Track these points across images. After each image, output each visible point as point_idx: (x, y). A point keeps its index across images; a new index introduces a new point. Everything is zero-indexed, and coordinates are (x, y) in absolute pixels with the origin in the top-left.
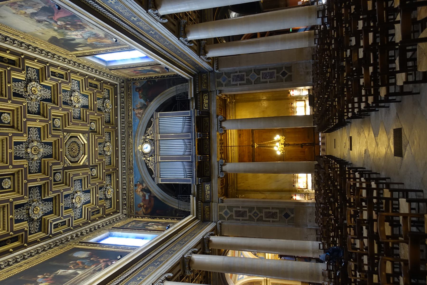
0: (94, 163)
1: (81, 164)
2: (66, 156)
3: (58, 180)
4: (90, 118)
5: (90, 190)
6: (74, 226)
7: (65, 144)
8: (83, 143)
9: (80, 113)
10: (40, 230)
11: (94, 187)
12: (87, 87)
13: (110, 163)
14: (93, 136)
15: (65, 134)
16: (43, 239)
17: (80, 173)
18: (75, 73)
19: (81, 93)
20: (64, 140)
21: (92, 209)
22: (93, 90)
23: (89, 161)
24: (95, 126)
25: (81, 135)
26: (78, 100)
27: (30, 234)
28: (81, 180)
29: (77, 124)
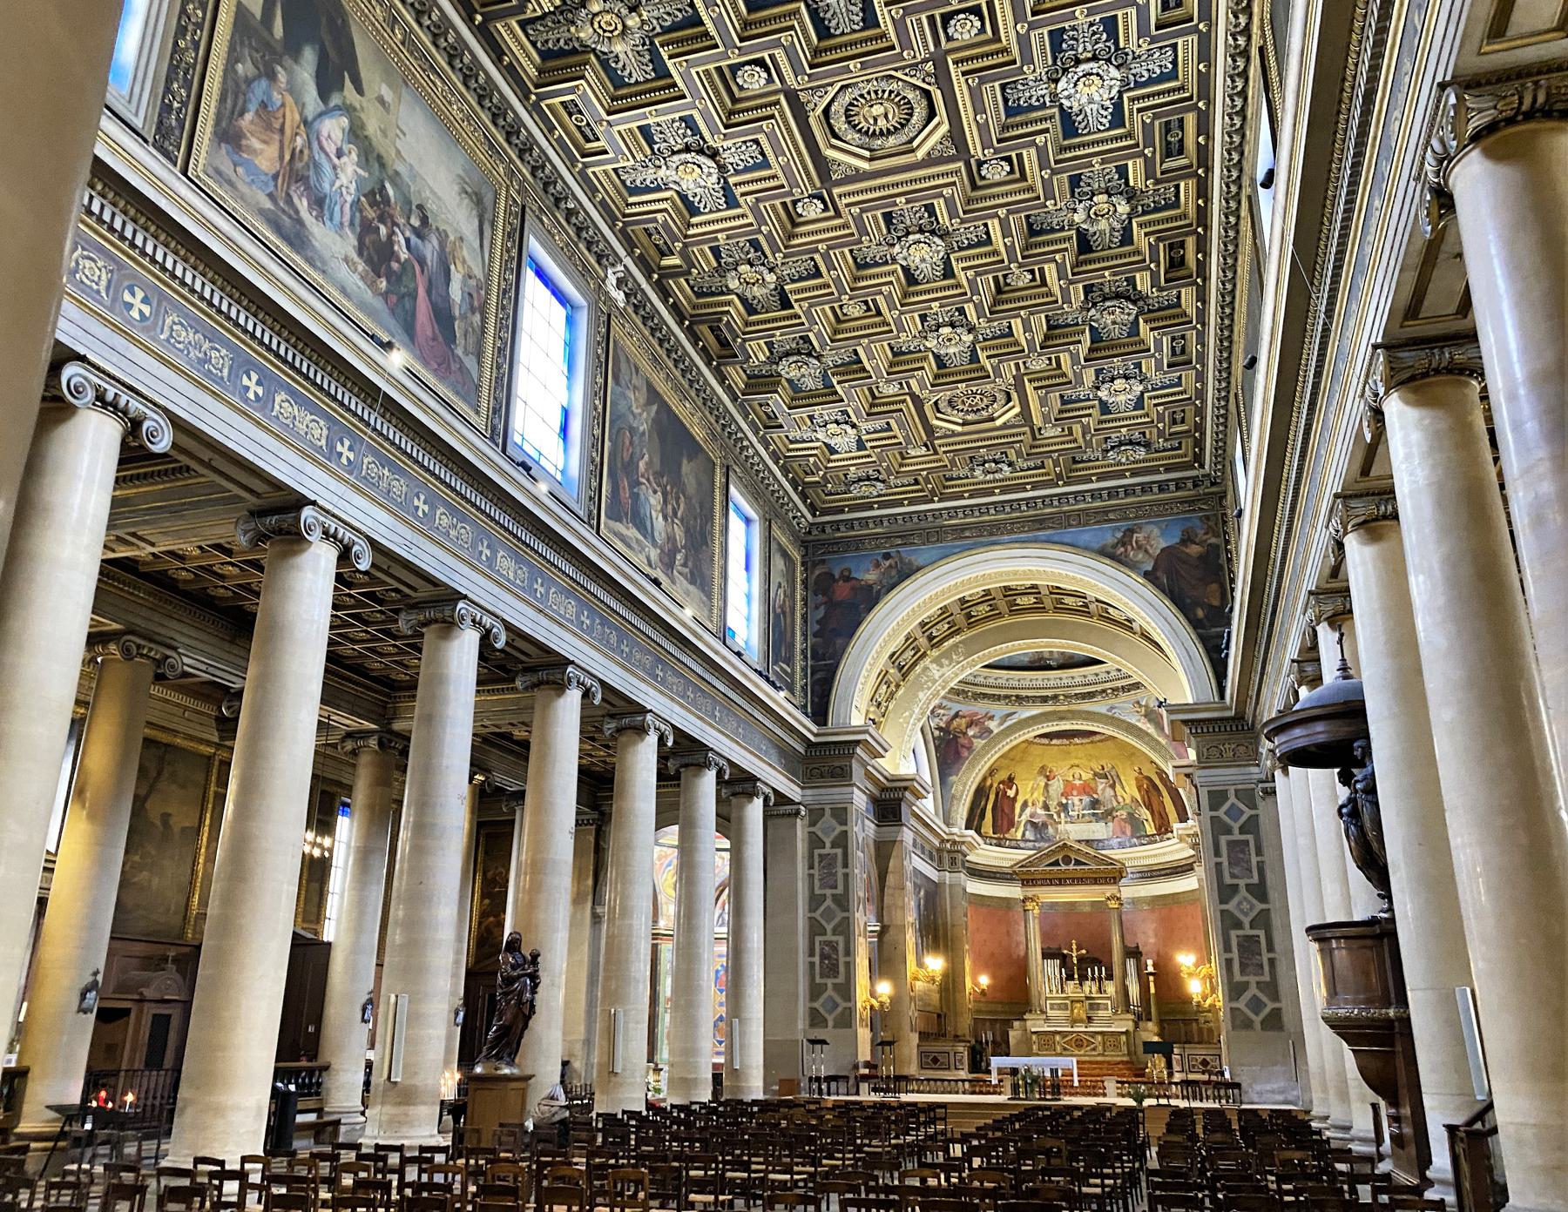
0: (845, 201)
1: (830, 153)
2: (842, 87)
3: (740, 81)
4: (1025, 153)
5: (739, 206)
6: (589, 171)
7: (892, 77)
8: (915, 144)
9: (1032, 108)
10: (546, 55)
11: (751, 219)
12: (1156, 117)
13: (867, 266)
14: (951, 180)
15: (929, 67)
16: (511, 72)
17: (789, 157)
18: (1205, 53)
19: (1125, 96)
20: (903, 68)
21: (665, 225)
22: (1149, 142)
23: (848, 180)
24: (997, 177)
25: (945, 128)
26: (1090, 93)
27: (523, 25)
28: (765, 165)
29: (979, 108)
